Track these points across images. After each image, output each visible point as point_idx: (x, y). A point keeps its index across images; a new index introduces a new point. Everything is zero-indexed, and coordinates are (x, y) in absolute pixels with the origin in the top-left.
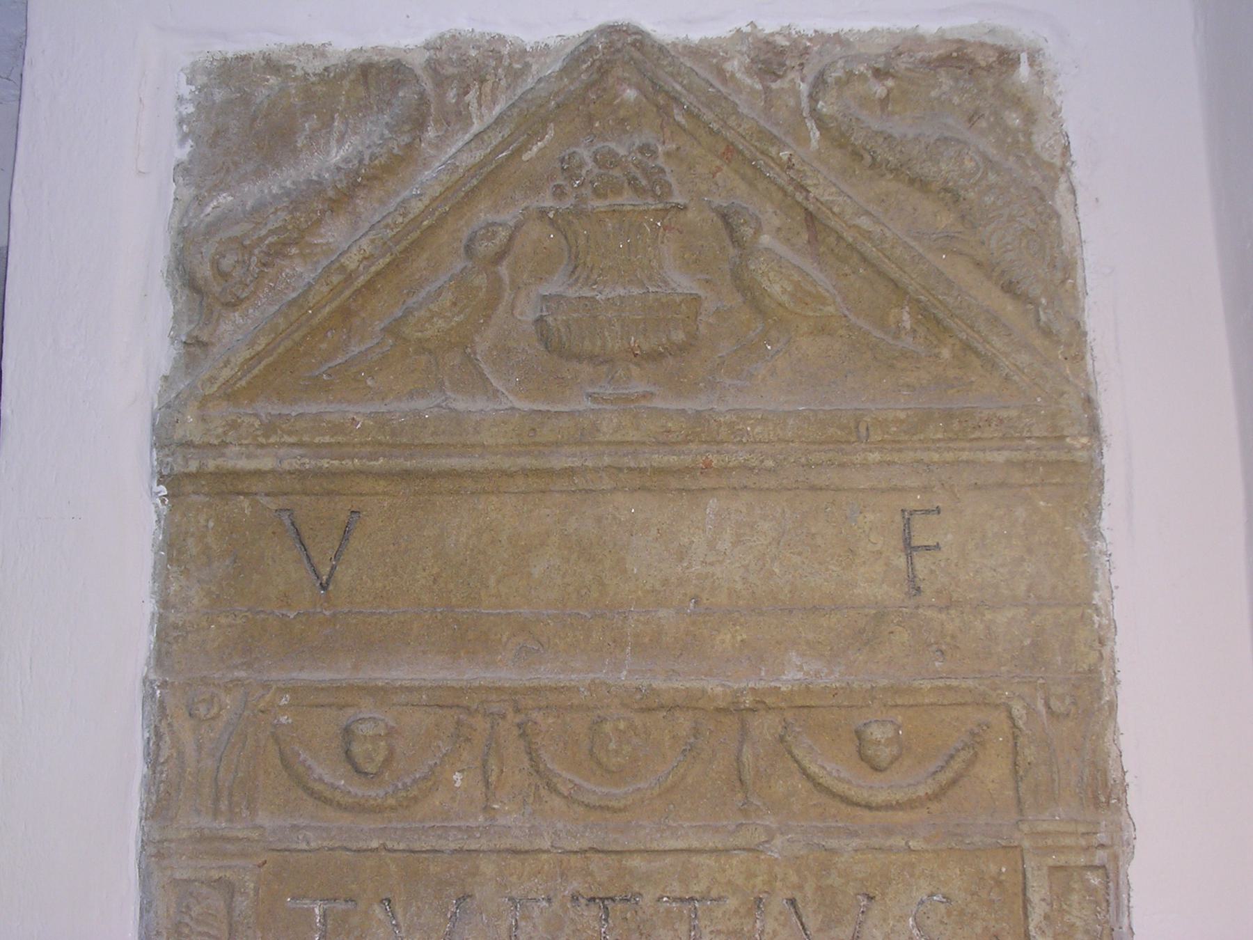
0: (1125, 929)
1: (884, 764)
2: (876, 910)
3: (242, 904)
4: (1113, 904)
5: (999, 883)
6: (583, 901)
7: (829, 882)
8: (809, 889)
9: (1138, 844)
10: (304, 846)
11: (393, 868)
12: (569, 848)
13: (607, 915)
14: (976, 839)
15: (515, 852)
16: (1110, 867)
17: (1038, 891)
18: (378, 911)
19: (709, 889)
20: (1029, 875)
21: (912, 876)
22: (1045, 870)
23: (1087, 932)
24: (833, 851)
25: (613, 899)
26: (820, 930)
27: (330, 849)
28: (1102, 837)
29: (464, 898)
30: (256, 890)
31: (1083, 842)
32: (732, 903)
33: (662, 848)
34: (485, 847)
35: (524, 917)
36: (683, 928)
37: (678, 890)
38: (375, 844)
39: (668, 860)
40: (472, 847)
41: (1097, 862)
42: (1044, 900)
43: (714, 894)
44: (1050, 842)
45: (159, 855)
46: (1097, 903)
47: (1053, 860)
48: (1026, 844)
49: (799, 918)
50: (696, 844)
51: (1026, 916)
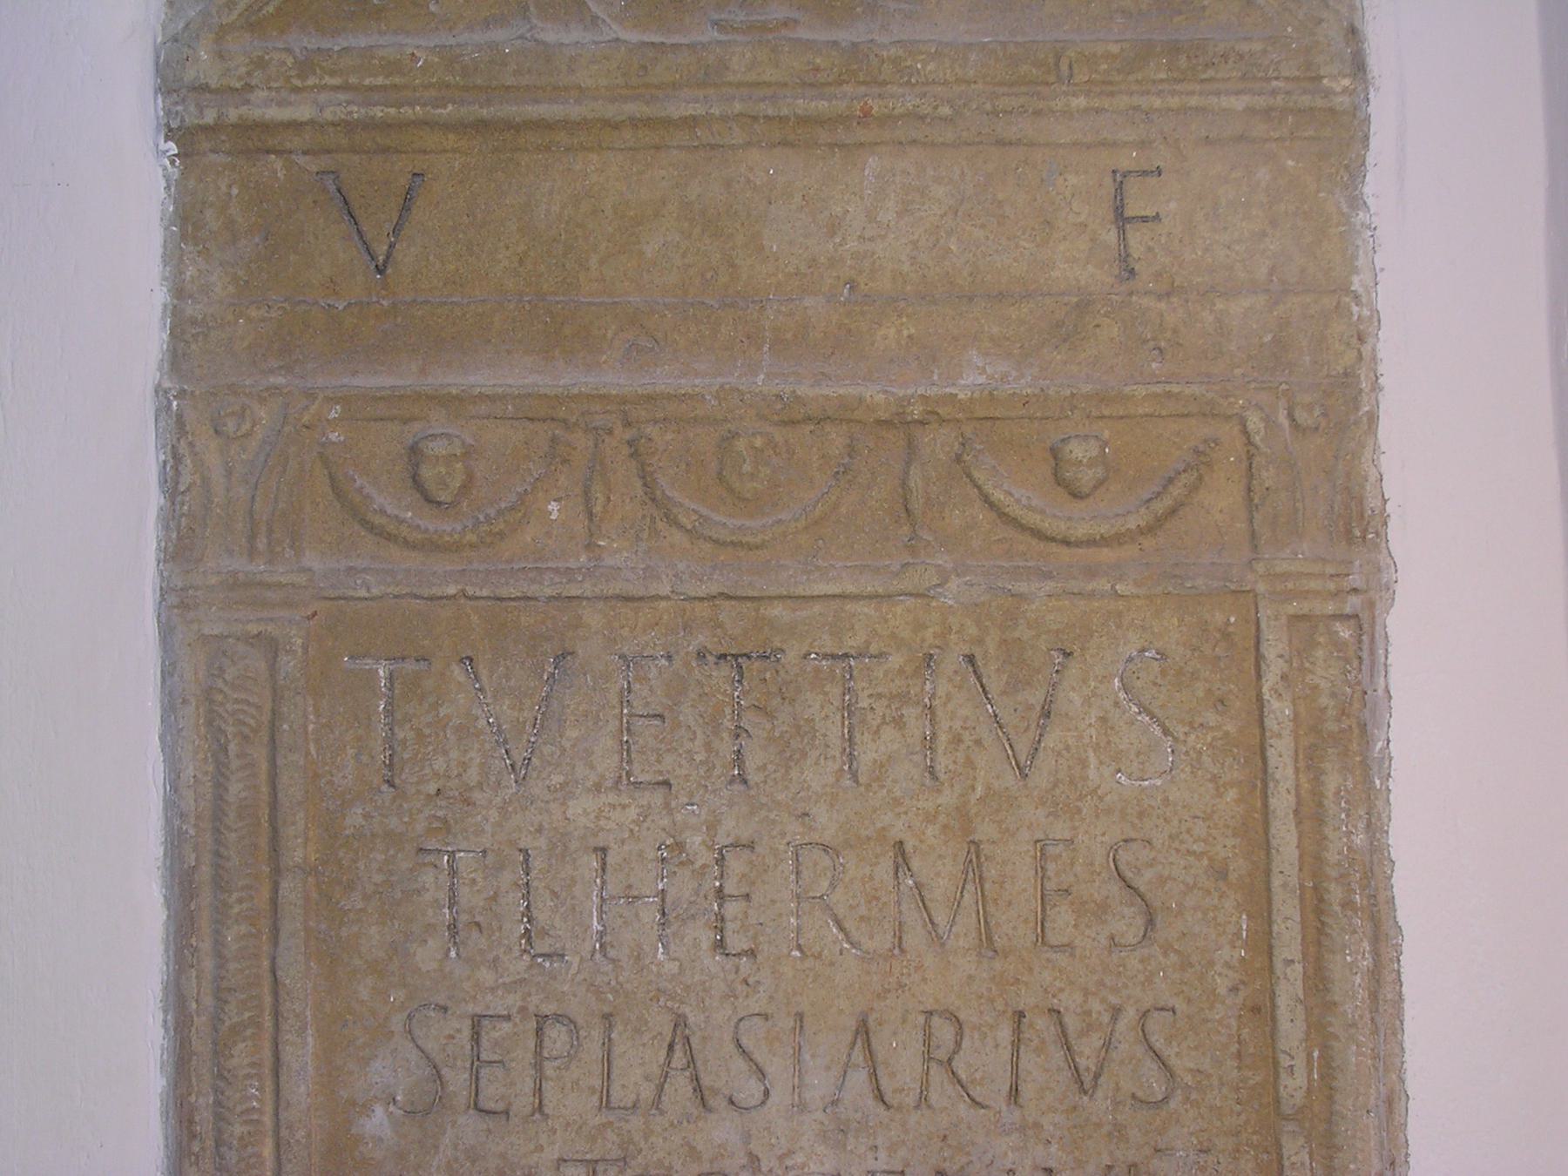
0: (1380, 692)
1: (1086, 490)
2: (1074, 670)
3: (288, 664)
4: (1366, 662)
5: (1226, 636)
6: (711, 659)
7: (1017, 634)
8: (991, 645)
9: (1399, 589)
10: (363, 593)
11: (475, 618)
12: (693, 594)
13: (742, 676)
14: (1200, 582)
15: (628, 599)
16: (1364, 616)
17: (1275, 647)
18: (457, 672)
19: (868, 643)
20: (1263, 625)
21: (1119, 627)
22: (1284, 620)
23: (1333, 695)
24: (1021, 597)
25: (749, 658)
26: (1004, 693)
27: (396, 597)
28: (1356, 580)
29: (563, 656)
30: (305, 648)
31: (1332, 586)
32: (896, 660)
33: (808, 593)
34: (588, 593)
35: (637, 679)
36: (835, 691)
37: (829, 646)
38: (451, 590)
39: (817, 608)
40: (574, 593)
41: (1348, 610)
42: (1281, 656)
43: (874, 649)
44: (1290, 585)
45: (183, 606)
46: (1347, 661)
47: (1294, 607)
48: (1261, 587)
49: (979, 678)
50: (851, 589)
51: (1259, 676)
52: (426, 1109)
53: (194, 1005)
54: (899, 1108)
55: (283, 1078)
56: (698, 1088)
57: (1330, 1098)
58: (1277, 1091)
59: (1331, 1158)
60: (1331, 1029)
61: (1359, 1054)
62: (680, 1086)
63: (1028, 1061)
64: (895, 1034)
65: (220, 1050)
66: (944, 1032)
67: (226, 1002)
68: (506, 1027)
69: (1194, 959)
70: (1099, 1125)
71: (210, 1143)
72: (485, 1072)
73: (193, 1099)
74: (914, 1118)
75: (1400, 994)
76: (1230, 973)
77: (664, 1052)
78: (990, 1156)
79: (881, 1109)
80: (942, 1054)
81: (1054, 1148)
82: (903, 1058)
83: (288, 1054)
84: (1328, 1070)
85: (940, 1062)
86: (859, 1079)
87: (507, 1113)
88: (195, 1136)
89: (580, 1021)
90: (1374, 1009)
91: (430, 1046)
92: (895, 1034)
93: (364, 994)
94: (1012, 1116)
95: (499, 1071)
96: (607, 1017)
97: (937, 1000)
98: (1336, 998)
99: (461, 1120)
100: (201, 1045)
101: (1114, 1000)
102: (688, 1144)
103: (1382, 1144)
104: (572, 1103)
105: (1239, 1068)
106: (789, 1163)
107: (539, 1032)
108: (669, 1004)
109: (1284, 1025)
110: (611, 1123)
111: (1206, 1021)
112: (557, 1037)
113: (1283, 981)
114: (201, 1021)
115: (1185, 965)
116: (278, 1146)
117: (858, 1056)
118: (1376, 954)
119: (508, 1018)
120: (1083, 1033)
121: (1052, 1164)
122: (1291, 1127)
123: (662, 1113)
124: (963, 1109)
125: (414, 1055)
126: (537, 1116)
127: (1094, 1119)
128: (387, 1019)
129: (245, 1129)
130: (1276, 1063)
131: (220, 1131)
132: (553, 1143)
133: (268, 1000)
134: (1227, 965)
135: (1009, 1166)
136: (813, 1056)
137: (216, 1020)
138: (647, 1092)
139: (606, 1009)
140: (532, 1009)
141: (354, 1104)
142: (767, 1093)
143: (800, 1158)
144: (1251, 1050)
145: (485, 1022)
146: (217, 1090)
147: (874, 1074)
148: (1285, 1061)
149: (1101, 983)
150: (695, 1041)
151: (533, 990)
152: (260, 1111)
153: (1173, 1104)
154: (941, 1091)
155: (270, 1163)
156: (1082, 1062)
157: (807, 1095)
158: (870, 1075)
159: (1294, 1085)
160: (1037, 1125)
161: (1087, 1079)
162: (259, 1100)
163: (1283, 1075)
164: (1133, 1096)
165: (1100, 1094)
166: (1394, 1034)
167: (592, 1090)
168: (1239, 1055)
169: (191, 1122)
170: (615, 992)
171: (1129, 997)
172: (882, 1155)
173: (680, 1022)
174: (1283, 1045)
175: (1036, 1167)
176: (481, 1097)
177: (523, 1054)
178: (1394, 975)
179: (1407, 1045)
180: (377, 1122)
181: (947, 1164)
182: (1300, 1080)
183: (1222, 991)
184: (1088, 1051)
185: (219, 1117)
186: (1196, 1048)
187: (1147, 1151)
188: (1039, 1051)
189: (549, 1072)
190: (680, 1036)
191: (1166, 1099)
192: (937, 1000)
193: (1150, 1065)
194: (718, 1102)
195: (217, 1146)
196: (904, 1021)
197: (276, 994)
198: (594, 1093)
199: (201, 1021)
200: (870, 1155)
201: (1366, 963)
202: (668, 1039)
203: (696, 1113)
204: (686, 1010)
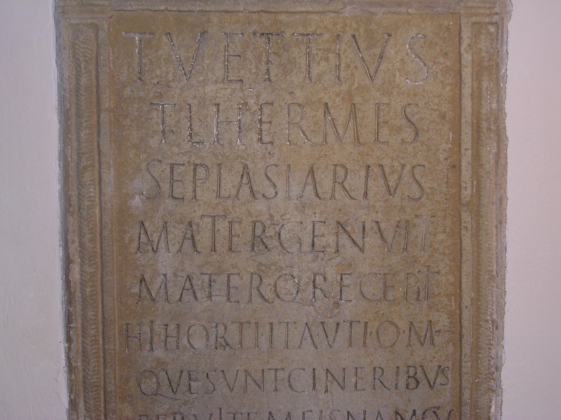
0: (504, 51)
2: (392, 41)
3: (102, 35)
4: (500, 41)
5: (448, 29)
6: (258, 35)
7: (371, 27)
8: (362, 30)
9: (513, 13)
10: (130, 8)
11: (171, 18)
12: (252, 10)
13: (269, 41)
14: (439, 9)
15: (227, 12)
16: (500, 23)
17: (466, 34)
18: (165, 39)
19: (316, 30)
20: (462, 26)
21: (409, 25)
22: (470, 24)
23: (487, 52)
24: (373, 14)
25: (272, 34)
26: (366, 49)
27: (142, 10)
28: (497, 10)
29: (203, 33)
30: (109, 29)
31: (488, 12)
32: (326, 36)
33: (294, 10)
34: (213, 10)
35: (231, 42)
36: (304, 47)
37: (302, 30)
38: (162, 8)
39: (298, 16)
40: (207, 10)
41: (494, 21)
42: (468, 37)
43: (318, 32)
44: (473, 11)
45: (63, 13)
46: (493, 40)
47: (474, 19)
48: (462, 12)
49: (357, 43)
50: (310, 9)
51: (460, 45)
52: (154, 197)
53: (70, 159)
56: (252, 191)
57: (479, 198)
58: (460, 195)
59: (479, 220)
60: (481, 174)
62: (246, 190)
65: (80, 175)
66: (341, 172)
67: (82, 158)
69: (432, 148)
70: (395, 207)
71: (77, 208)
72: (174, 184)
74: (329, 203)
75: (506, 162)
76: (445, 153)
77: (240, 178)
78: (356, 216)
79: (318, 199)
80: (340, 180)
81: (379, 214)
82: (326, 182)
83: (104, 176)
85: (339, 183)
86: (310, 189)
87: (183, 198)
89: (209, 166)
91: (155, 174)
92: (323, 172)
95: (180, 184)
96: (219, 165)
97: (338, 161)
98: (483, 163)
99: (167, 201)
100: (73, 173)
101: (402, 162)
102: (248, 210)
103: (497, 215)
105: (447, 187)
106: (284, 218)
107: (195, 170)
108: (242, 160)
109: (464, 172)
110: (220, 203)
111: (436, 170)
112: (201, 172)
113: (464, 156)
115: (429, 150)
116: (101, 209)
117: (310, 180)
118: (498, 147)
119: (184, 165)
120: (392, 173)
121: (378, 220)
122: (465, 208)
123: (239, 199)
124: (347, 200)
125: (149, 178)
127: (394, 204)
129: (89, 203)
130: (460, 186)
132: (200, 210)
134: (444, 150)
136: (293, 180)
137: (78, 164)
138: (234, 192)
139: (219, 162)
140: (192, 161)
141: (128, 194)
142: (277, 193)
143: (288, 216)
145: (175, 166)
146: (79, 190)
147: (315, 187)
148: (464, 185)
150: (251, 174)
153: (423, 200)
154: (339, 193)
155: (98, 216)
156: (391, 184)
157: (291, 194)
159: (467, 193)
160: (373, 206)
161: (392, 190)
163: (463, 190)
164: (409, 196)
165: (396, 195)
166: (503, 176)
168: (447, 182)
169: (70, 200)
170: (222, 156)
172: (317, 215)
173: (245, 167)
174: (463, 179)
175: (372, 221)
176: (174, 192)
178: (504, 155)
179: (508, 180)
180: (137, 202)
182: (469, 192)
183: (442, 159)
184: (392, 180)
185: (79, 199)
186: (432, 180)
188: (375, 180)
189: (198, 184)
191: (420, 198)
192: (338, 161)
193: (415, 186)
194: (259, 196)
196: (326, 168)
197: (99, 155)
198: (214, 192)
200: (313, 216)
201: (494, 151)
202: (241, 173)
204: (248, 163)
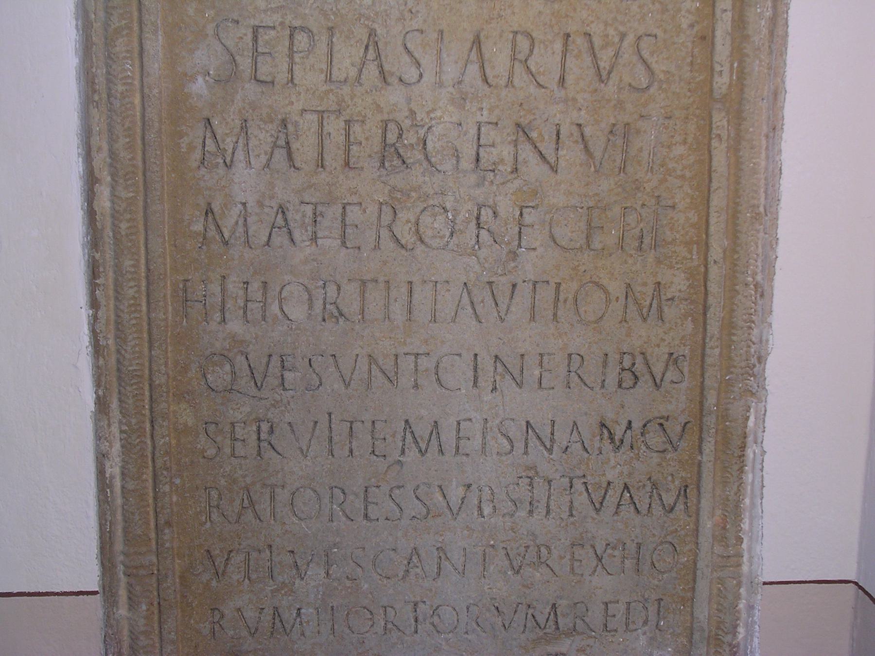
52: (227, 80)
53: (93, 16)
54: (496, 87)
55: (145, 59)
56: (382, 72)
57: (742, 90)
58: (712, 85)
59: (740, 125)
60: (745, 51)
61: (760, 66)
62: (372, 69)
63: (571, 62)
64: (495, 43)
65: (109, 42)
66: (523, 44)
67: (112, 14)
68: (273, 33)
69: (670, 7)
70: (609, 101)
71: (104, 96)
72: (260, 59)
73: (94, 70)
74: (504, 93)
75: (787, 32)
76: (690, 17)
77: (362, 50)
78: (546, 115)
79: (486, 87)
80: (522, 57)
81: (583, 113)
82: (499, 59)
83: (148, 45)
84: (741, 76)
85: (521, 61)
86: (473, 69)
87: (273, 83)
88: (95, 92)
89: (315, 31)
90: (771, 41)
91: (230, 43)
92: (495, 43)
93: (191, 11)
94: (560, 94)
95: (268, 59)
96: (331, 29)
97: (520, 25)
98: (750, 33)
99: (247, 86)
100: (97, 39)
101: (622, 29)
102: (375, 103)
103: (769, 118)
104: (309, 77)
105: (691, 71)
106: (432, 115)
107: (291, 36)
108: (366, 22)
109: (719, 47)
110: (332, 90)
111: (674, 43)
112: (302, 40)
113: (719, 22)
114: (97, 26)
115: (664, 10)
116: (143, 97)
117: (474, 56)
118: (775, 7)
119: (274, 28)
120: (604, 47)
121: (581, 122)
122: (718, 106)
123: (361, 85)
124: (532, 89)
125: (220, 48)
126: (290, 84)
127: (607, 97)
128: (204, 27)
129: (124, 88)
130: (712, 69)
131: (110, 89)
132: (298, 101)
133: (136, 14)
134: (688, 11)
135: (557, 122)
136: (448, 55)
137: (106, 25)
138: (353, 73)
139: (330, 25)
140: (287, 23)
141: (186, 75)
142: (421, 76)
143: (438, 113)
144: (699, 61)
145: (261, 30)
146: (108, 66)
147: (482, 67)
148: (718, 68)
149: (615, 19)
150: (380, 45)
151: (288, 13)
152: (133, 78)
153: (652, 90)
154: (520, 78)
155: (138, 109)
156: (602, 64)
157: (444, 78)
158: (480, 67)
159: (722, 82)
160: (574, 99)
161: (604, 74)
162: (132, 72)
163: (716, 76)
164: (630, 85)
165: (611, 83)
166: (781, 55)
167: (322, 71)
168: (692, 63)
169: (93, 83)
170: (334, 14)
171: (631, 28)
172: (485, 113)
173: (372, 33)
174: (717, 58)
175: (572, 123)
176: (258, 72)
177: (283, 48)
178: (784, 21)
179: (788, 62)
180: (199, 86)
181: (522, 119)
182: (725, 79)
183: (684, 26)
184: (605, 58)
185: (109, 81)
186: (667, 59)
187: (636, 116)
188: (577, 57)
189: (297, 60)
190: (372, 41)
191: (648, 88)
192: (520, 25)
193: (640, 68)
194: (393, 80)
195: (109, 98)
196: (501, 36)
197: (140, 10)
198: (322, 73)
199: (97, 26)
200: (479, 113)
201: (769, 14)
202: (365, 43)
203: (380, 86)
204: (376, 26)
